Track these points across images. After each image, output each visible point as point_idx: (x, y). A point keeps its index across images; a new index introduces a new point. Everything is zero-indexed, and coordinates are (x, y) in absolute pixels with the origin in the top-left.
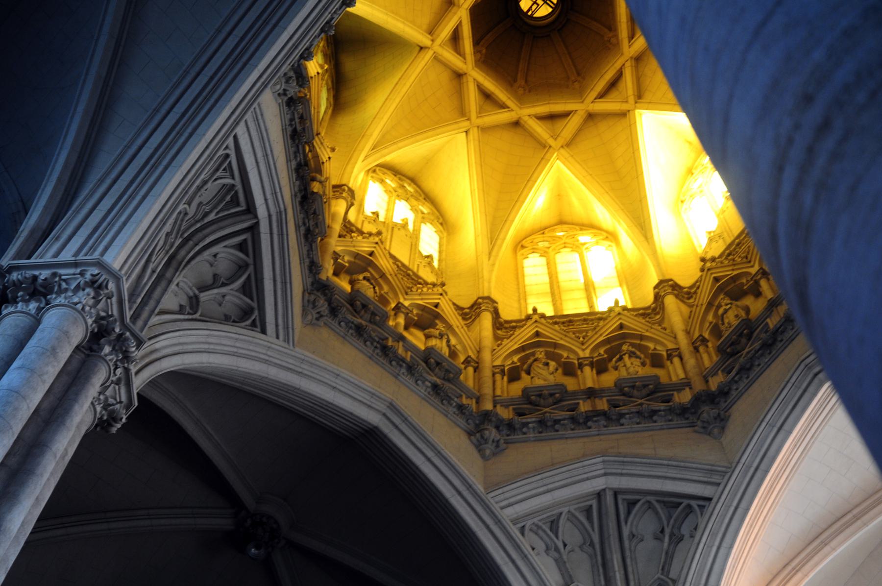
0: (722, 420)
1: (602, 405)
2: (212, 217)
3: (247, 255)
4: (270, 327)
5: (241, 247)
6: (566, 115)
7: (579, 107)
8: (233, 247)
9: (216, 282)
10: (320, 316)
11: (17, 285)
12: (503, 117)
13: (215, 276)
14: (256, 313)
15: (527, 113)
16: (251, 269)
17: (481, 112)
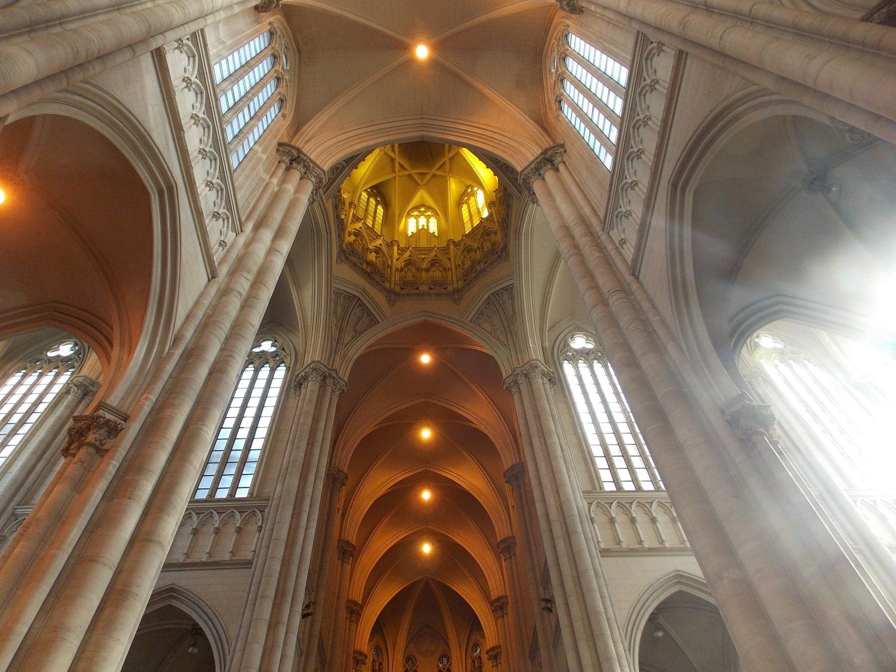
0: (508, 255)
2: (347, 305)
4: (380, 320)
5: (360, 304)
6: (445, 163)
8: (358, 307)
9: (360, 318)
10: (394, 301)
12: (428, 177)
13: (358, 318)
14: (374, 319)
15: (434, 171)
17: (422, 180)
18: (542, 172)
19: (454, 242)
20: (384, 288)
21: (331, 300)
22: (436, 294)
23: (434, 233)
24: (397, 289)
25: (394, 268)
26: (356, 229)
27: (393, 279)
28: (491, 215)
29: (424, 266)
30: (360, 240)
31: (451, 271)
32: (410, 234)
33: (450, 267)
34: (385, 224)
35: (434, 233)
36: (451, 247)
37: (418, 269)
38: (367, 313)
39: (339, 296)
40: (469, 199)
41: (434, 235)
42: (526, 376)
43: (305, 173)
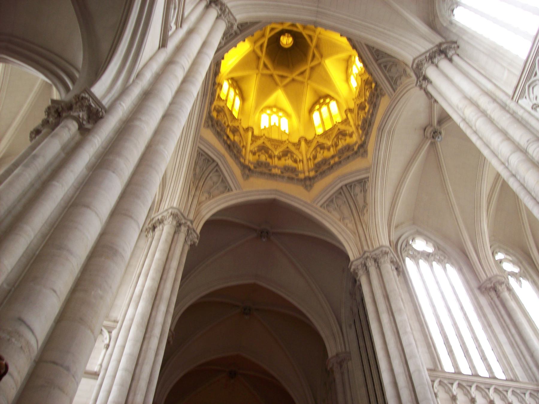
1: (336, 159)
5: (217, 171)
7: (307, 67)
9: (214, 183)
11: (155, 223)
12: (288, 80)
13: (214, 183)
14: (228, 187)
15: (294, 75)
16: (222, 176)
17: (281, 82)
18: (436, 60)
19: (306, 140)
24: (252, 167)
28: (345, 121)
31: (303, 162)
33: (301, 158)
36: (303, 143)
37: (270, 157)
38: (222, 180)
40: (320, 108)
42: (376, 260)
43: (220, 15)
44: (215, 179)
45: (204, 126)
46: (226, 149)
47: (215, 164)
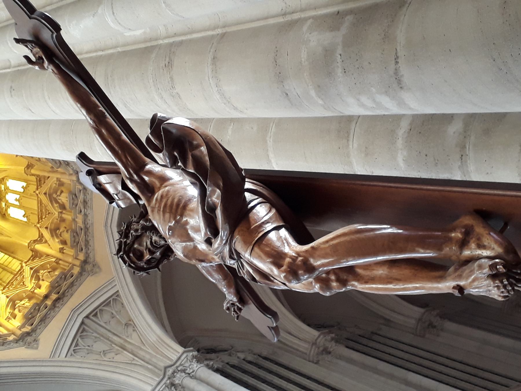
2: (95, 334)
3: (97, 312)
5: (95, 315)
8: (98, 318)
20: (80, 274)
21: (81, 362)
22: (84, 208)
23: (23, 187)
25: (59, 255)
26: (7, 306)
27: (70, 260)
29: (57, 213)
30: (21, 301)
32: (25, 219)
34: (12, 253)
35: (23, 187)
39: (83, 347)
41: (26, 188)
44: (106, 317)
45: (37, 348)
46: (63, 305)
47: (87, 321)
